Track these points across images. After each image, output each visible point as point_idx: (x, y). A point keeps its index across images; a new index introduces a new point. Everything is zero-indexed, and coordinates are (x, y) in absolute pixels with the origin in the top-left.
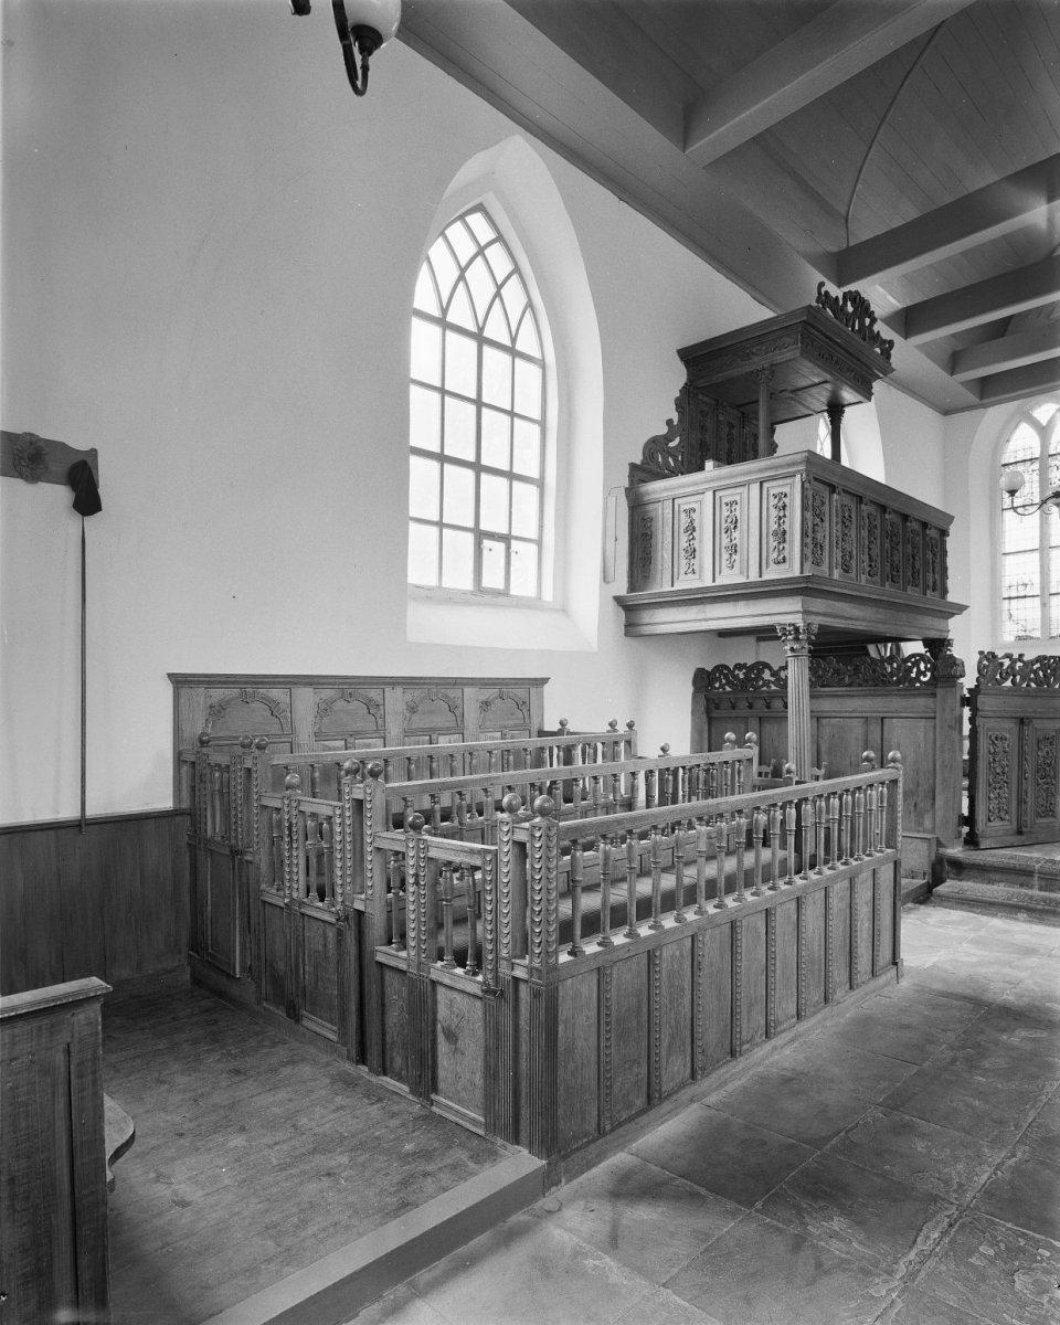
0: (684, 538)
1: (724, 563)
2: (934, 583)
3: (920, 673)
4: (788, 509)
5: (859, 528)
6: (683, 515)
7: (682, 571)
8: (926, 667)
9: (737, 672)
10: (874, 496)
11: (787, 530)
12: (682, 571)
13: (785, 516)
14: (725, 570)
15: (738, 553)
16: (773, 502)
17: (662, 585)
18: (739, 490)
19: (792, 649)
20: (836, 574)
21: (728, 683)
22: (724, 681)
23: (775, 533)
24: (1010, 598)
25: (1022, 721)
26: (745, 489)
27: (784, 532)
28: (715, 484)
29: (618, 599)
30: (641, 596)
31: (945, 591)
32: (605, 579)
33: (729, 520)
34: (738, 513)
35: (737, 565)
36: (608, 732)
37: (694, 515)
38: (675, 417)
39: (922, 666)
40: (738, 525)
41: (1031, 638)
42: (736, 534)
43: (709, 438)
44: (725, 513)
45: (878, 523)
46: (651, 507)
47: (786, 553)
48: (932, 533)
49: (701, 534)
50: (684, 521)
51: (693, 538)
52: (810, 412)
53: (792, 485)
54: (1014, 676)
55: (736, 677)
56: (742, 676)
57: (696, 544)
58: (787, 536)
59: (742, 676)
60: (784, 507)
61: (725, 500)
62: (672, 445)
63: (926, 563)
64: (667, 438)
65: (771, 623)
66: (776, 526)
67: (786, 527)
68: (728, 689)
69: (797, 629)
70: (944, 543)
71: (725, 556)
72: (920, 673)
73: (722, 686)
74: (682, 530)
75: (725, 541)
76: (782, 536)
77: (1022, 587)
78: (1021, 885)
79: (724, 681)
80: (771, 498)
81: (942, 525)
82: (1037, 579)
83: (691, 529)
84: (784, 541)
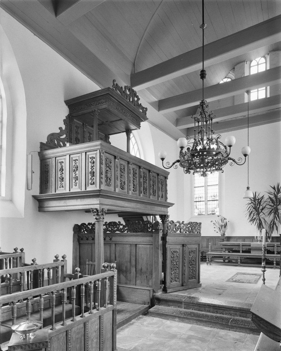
0: (59, 173)
1: (73, 184)
2: (162, 195)
4: (95, 163)
5: (129, 173)
6: (59, 164)
8: (150, 226)
10: (134, 162)
11: (95, 171)
12: (59, 186)
13: (94, 166)
14: (74, 186)
15: (78, 180)
16: (90, 160)
17: (52, 192)
20: (117, 190)
23: (91, 173)
24: (196, 202)
25: (183, 245)
26: (80, 155)
29: (34, 197)
30: (44, 196)
31: (166, 198)
32: (28, 188)
33: (75, 167)
34: (78, 164)
35: (78, 184)
36: (14, 253)
37: (63, 164)
38: (64, 127)
40: (78, 169)
42: (77, 172)
43: (79, 136)
44: (74, 164)
45: (137, 172)
46: (48, 160)
47: (94, 180)
48: (161, 177)
49: (65, 172)
50: (59, 166)
51: (63, 173)
52: (121, 132)
53: (96, 154)
54: (181, 229)
58: (95, 174)
60: (94, 162)
61: (74, 159)
62: (62, 137)
63: (158, 188)
64: (59, 135)
65: (89, 208)
66: (91, 170)
67: (94, 170)
69: (97, 211)
70: (166, 182)
71: (74, 181)
74: (59, 170)
75: (74, 175)
76: (93, 174)
77: (199, 198)
78: (179, 307)
80: (89, 159)
81: (166, 176)
82: (204, 196)
83: (62, 170)
84: (94, 176)
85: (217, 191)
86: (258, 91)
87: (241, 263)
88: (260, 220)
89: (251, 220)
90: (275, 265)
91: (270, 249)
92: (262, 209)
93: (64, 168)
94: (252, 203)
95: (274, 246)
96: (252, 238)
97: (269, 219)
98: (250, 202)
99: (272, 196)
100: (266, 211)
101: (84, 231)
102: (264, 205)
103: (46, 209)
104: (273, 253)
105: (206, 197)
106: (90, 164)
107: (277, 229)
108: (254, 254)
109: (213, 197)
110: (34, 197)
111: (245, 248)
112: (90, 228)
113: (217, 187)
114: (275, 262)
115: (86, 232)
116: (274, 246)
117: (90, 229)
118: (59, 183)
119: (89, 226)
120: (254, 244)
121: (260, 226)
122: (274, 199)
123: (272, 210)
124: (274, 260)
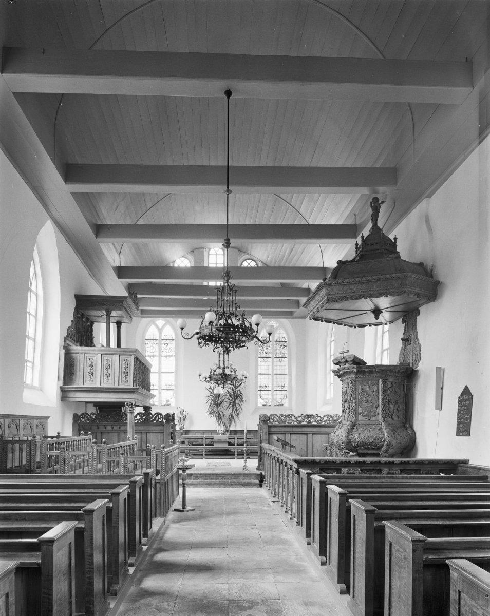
1: (105, 380)
3: (159, 419)
6: (88, 360)
11: (129, 372)
14: (105, 382)
17: (79, 383)
18: (111, 356)
19: (130, 410)
28: (103, 352)
29: (60, 387)
32: (58, 380)
39: (160, 416)
41: (155, 405)
42: (109, 370)
47: (128, 379)
49: (96, 367)
50: (89, 363)
57: (94, 371)
60: (128, 365)
69: (132, 404)
71: (105, 377)
72: (159, 419)
80: (123, 361)
83: (92, 366)
86: (216, 264)
87: (206, 455)
88: (219, 413)
89: (210, 413)
90: (236, 455)
91: (232, 441)
92: (221, 402)
93: (93, 364)
94: (211, 395)
95: (234, 438)
96: (214, 431)
97: (227, 412)
98: (210, 395)
99: (230, 391)
100: (225, 404)
101: (85, 421)
102: (223, 399)
103: (71, 399)
104: (234, 445)
105: (160, 386)
106: (124, 366)
107: (235, 422)
108: (216, 446)
109: (168, 386)
110: (60, 387)
111: (208, 441)
112: (94, 417)
113: (173, 375)
114: (236, 453)
115: (88, 422)
116: (234, 438)
117: (94, 419)
119: (92, 416)
120: (216, 437)
121: (219, 418)
122: (232, 393)
123: (230, 403)
124: (236, 451)
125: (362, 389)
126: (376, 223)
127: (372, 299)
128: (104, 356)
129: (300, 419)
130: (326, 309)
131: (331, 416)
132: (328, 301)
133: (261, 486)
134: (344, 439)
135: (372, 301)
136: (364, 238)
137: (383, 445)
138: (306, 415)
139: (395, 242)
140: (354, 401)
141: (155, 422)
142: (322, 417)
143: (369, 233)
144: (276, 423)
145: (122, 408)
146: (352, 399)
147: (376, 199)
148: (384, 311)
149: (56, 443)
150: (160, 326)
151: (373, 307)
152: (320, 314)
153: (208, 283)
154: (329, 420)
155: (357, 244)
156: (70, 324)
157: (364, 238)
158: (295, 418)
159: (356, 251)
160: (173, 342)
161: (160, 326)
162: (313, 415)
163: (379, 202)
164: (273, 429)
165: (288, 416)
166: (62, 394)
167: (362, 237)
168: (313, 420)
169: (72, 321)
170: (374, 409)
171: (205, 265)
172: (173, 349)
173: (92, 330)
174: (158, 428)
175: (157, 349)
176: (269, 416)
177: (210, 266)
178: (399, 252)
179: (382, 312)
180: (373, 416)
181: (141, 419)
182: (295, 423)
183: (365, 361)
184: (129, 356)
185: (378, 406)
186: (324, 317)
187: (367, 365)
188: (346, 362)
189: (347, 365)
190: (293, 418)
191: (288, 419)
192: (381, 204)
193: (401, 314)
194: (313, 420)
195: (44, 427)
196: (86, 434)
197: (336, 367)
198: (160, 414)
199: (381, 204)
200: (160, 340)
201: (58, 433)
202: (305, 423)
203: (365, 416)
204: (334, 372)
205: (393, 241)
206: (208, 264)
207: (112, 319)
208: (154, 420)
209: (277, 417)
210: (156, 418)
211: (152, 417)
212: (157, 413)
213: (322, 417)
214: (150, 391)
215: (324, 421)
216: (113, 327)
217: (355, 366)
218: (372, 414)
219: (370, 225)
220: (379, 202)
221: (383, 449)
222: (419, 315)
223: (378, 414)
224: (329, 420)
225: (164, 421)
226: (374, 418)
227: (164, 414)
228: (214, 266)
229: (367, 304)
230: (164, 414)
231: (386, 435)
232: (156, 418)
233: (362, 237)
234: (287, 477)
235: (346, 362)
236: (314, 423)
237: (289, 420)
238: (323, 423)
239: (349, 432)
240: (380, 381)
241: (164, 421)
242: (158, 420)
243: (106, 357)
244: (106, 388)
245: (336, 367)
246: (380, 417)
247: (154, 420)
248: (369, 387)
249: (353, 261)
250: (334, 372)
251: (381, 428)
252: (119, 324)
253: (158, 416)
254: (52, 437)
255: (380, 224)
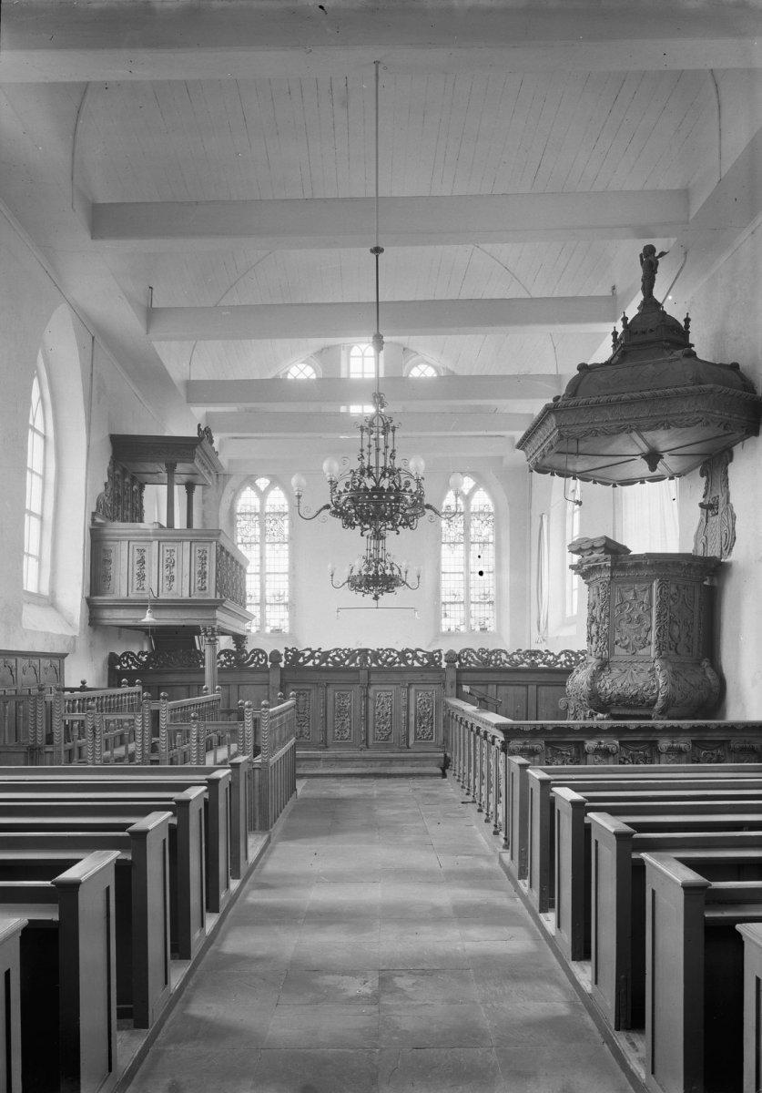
3: (259, 659)
7: (135, 587)
9: (140, 657)
12: (135, 587)
18: (176, 544)
21: (135, 664)
22: (130, 663)
23: (200, 573)
27: (205, 573)
37: (145, 554)
39: (260, 656)
44: (166, 557)
47: (207, 584)
50: (137, 556)
55: (140, 660)
56: (144, 659)
57: (146, 572)
59: (144, 659)
60: (205, 558)
61: (166, 548)
65: (195, 623)
68: (133, 668)
69: (213, 629)
73: (128, 666)
76: (203, 575)
79: (130, 663)
83: (142, 562)
85: (286, 585)
86: (363, 373)
103: (106, 622)
106: (199, 561)
109: (277, 598)
118: (136, 581)
125: (622, 597)
126: (651, 293)
127: (643, 433)
128: (164, 543)
129: (516, 657)
130: (557, 453)
131: (572, 652)
132: (561, 437)
133: (444, 775)
134: (585, 687)
135: (641, 437)
136: (629, 322)
137: (655, 701)
138: (528, 651)
139: (687, 326)
140: (607, 620)
141: (252, 665)
142: (556, 654)
143: (637, 312)
144: (473, 665)
145: (196, 637)
146: (603, 615)
147: (649, 250)
148: (665, 455)
149: (79, 700)
150: (263, 488)
151: (645, 449)
152: (546, 461)
153: (348, 409)
154: (570, 661)
155: (615, 334)
156: (101, 489)
157: (629, 322)
158: (508, 656)
159: (614, 346)
160: (286, 517)
161: (263, 488)
162: (539, 651)
163: (657, 254)
164: (465, 676)
165: (494, 652)
166: (90, 612)
167: (625, 319)
168: (540, 661)
169: (106, 484)
170: (643, 635)
171: (343, 375)
172: (286, 532)
173: (141, 498)
174: (259, 677)
175: (258, 531)
176: (457, 652)
177: (352, 376)
178: (693, 345)
179: (661, 457)
180: (641, 648)
181: (227, 660)
182: (507, 665)
183: (629, 547)
184: (208, 544)
185: (650, 629)
186: (556, 465)
187: (631, 553)
188: (593, 548)
189: (596, 555)
190: (504, 657)
191: (493, 658)
192: (658, 257)
193: (697, 459)
194: (540, 661)
195: (59, 673)
196: (131, 684)
197: (576, 558)
198: (262, 652)
199: (658, 257)
200: (262, 516)
201: (83, 683)
202: (525, 665)
203: (626, 647)
204: (572, 567)
205: (683, 324)
206: (349, 372)
207: (177, 479)
208: (251, 662)
209: (473, 654)
210: (253, 658)
211: (248, 656)
212: (255, 650)
213: (556, 654)
214: (245, 607)
215: (561, 663)
216: (179, 491)
217: (609, 556)
218: (639, 644)
219: (640, 297)
220: (657, 254)
221: (656, 707)
222: (731, 461)
223: (650, 644)
224: (570, 661)
225: (269, 664)
226: (641, 652)
227: (268, 653)
228: (359, 376)
229: (632, 445)
230: (268, 653)
231: (661, 681)
232: (253, 658)
233: (625, 319)
234: (488, 758)
235: (593, 548)
236: (542, 665)
237: (496, 660)
238: (559, 666)
239: (595, 677)
240: (655, 584)
241: (269, 664)
242: (257, 663)
243: (168, 546)
244: (167, 601)
245: (576, 558)
246: (653, 650)
247: (251, 662)
248: (635, 595)
249: (607, 363)
250: (572, 567)
251: (653, 670)
252: (190, 487)
253: (257, 655)
254: (72, 690)
255: (658, 294)
